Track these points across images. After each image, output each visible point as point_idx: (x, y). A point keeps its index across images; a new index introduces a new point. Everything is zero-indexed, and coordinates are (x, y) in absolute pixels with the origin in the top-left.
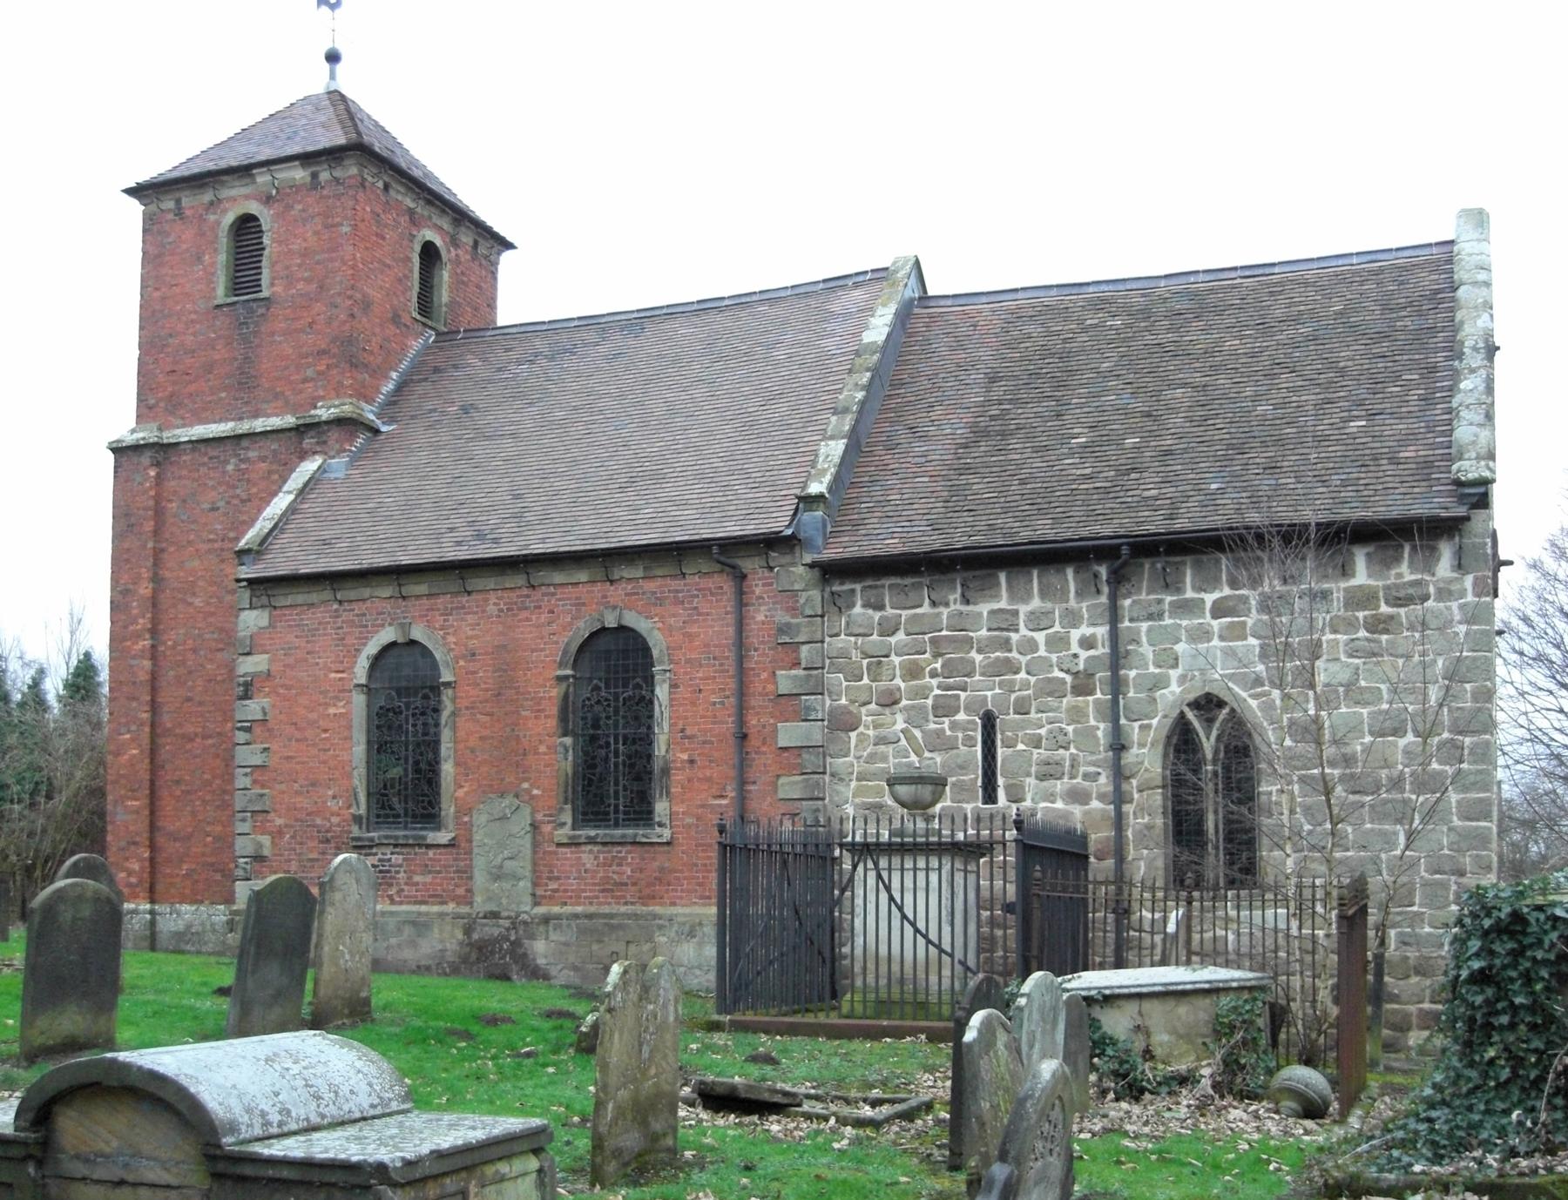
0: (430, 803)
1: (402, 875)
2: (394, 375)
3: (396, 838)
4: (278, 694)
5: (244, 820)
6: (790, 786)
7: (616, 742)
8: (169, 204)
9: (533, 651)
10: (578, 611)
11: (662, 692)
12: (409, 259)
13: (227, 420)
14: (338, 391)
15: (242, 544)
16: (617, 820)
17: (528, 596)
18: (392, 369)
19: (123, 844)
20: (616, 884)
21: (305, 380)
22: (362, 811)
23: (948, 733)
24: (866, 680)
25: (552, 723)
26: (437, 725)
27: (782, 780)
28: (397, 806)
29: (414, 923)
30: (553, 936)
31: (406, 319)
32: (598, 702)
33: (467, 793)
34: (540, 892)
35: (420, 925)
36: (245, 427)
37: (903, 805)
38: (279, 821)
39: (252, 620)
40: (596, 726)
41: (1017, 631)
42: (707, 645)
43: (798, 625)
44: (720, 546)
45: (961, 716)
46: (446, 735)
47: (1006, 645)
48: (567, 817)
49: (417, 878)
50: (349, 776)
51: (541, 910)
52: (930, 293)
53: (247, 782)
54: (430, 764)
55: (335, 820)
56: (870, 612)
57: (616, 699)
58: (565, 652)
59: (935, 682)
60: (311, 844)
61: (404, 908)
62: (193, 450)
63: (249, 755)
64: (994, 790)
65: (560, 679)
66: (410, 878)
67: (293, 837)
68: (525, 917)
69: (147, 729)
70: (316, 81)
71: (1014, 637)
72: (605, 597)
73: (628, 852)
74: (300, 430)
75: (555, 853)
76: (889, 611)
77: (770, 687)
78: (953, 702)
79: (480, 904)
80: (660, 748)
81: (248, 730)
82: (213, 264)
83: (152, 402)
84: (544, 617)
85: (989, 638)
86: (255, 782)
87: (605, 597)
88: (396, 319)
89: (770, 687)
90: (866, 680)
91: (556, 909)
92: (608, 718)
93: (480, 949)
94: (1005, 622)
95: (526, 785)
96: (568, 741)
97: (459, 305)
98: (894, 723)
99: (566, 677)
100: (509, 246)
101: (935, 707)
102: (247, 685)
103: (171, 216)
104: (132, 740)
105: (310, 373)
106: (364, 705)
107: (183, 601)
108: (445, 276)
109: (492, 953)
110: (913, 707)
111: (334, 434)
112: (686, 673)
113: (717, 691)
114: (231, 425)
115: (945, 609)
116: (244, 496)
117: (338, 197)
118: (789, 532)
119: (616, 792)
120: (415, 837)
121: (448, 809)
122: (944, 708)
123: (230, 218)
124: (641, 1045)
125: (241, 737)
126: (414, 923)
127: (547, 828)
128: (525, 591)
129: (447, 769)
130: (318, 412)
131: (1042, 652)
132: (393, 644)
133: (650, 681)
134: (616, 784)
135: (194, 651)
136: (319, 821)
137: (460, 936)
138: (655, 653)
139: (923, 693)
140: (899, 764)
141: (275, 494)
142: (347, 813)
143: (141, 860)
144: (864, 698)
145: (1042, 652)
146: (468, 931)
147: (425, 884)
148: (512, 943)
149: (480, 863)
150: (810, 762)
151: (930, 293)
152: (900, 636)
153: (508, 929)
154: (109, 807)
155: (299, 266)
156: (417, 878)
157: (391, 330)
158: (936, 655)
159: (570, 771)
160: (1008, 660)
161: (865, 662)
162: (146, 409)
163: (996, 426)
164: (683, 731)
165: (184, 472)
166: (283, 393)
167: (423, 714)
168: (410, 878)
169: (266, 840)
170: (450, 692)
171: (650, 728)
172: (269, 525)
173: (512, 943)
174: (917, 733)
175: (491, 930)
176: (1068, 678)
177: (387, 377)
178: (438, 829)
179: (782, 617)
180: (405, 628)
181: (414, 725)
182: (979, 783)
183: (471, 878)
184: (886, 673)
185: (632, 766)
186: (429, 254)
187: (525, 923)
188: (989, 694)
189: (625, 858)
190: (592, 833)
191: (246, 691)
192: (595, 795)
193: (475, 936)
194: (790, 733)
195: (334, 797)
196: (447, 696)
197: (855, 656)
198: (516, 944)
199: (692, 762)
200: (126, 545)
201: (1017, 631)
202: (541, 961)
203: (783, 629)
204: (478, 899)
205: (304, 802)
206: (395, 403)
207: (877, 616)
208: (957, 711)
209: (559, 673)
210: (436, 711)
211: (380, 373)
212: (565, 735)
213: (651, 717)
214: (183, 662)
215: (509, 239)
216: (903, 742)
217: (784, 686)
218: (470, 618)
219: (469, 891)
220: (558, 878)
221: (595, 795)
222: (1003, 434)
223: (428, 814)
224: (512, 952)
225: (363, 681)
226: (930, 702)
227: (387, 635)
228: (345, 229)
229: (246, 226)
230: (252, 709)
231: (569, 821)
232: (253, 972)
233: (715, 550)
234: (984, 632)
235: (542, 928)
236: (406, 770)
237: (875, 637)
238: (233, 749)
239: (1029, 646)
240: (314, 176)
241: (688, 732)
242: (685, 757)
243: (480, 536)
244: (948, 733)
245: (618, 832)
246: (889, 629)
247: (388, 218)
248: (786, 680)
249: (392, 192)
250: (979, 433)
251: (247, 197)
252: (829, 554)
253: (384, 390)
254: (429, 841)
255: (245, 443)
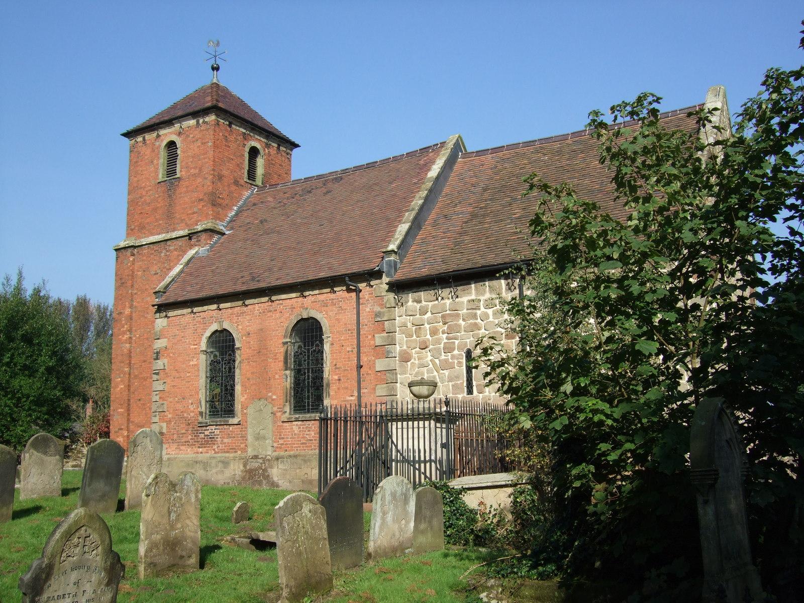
0: (231, 405)
1: (219, 439)
2: (235, 208)
3: (216, 422)
4: (170, 357)
5: (155, 416)
6: (381, 390)
7: (308, 372)
8: (140, 139)
9: (274, 331)
10: (292, 311)
11: (327, 347)
12: (243, 155)
13: (162, 233)
14: (207, 216)
15: (157, 290)
16: (309, 409)
17: (271, 306)
18: (233, 205)
19: (117, 429)
20: (308, 440)
21: (194, 213)
22: (203, 409)
23: (450, 361)
24: (415, 337)
25: (281, 364)
26: (234, 368)
27: (379, 386)
28: (218, 407)
29: (223, 462)
30: (280, 466)
31: (242, 182)
32: (301, 354)
33: (246, 399)
34: (275, 445)
35: (226, 464)
36: (168, 236)
37: (414, 395)
38: (170, 416)
39: (161, 322)
40: (300, 365)
41: (479, 309)
42: (346, 324)
43: (383, 312)
44: (349, 277)
45: (456, 352)
46: (237, 372)
47: (475, 316)
48: (287, 409)
49: (226, 440)
50: (197, 393)
51: (275, 454)
52: (468, 151)
53: (157, 398)
54: (232, 387)
55: (192, 414)
56: (415, 304)
57: (308, 352)
58: (286, 332)
59: (445, 336)
60: (182, 426)
61: (219, 455)
62: (148, 248)
63: (158, 386)
64: (472, 387)
65: (285, 343)
66: (222, 441)
67: (175, 423)
68: (269, 457)
69: (127, 376)
70: (207, 78)
71: (479, 312)
72: (303, 304)
73: (313, 425)
74: (190, 236)
75: (282, 426)
76: (424, 303)
77: (372, 342)
78: (452, 346)
79: (250, 452)
80: (326, 375)
81: (157, 374)
82: (157, 164)
83: (133, 227)
84: (278, 315)
85: (467, 313)
86: (160, 398)
87: (303, 304)
88: (236, 183)
89: (372, 342)
90: (415, 337)
91: (282, 453)
92: (305, 361)
93: (250, 473)
94: (474, 305)
95: (270, 394)
96: (288, 372)
97: (270, 174)
98: (427, 357)
99: (287, 343)
100: (297, 146)
101: (444, 349)
102: (158, 353)
103: (141, 144)
104: (121, 381)
105: (195, 210)
106: (205, 359)
107: (143, 316)
108: (260, 162)
109: (255, 475)
110: (435, 349)
111: (203, 236)
112: (337, 338)
113: (350, 346)
114: (164, 235)
115: (446, 299)
116: (168, 267)
117: (207, 130)
118: (377, 268)
119: (308, 396)
120: (224, 421)
121: (238, 407)
122: (448, 349)
123: (165, 143)
124: (169, 513)
125: (155, 377)
126: (223, 462)
127: (279, 414)
128: (270, 303)
129: (238, 388)
130: (198, 227)
131: (491, 319)
132: (216, 331)
133: (322, 341)
134: (308, 392)
135: (147, 339)
136: (185, 415)
137: (242, 467)
138: (324, 329)
139: (438, 342)
140: (430, 377)
141: (176, 265)
142: (197, 411)
143: (124, 437)
144: (413, 345)
145: (491, 319)
146: (245, 466)
147: (228, 443)
148: (263, 470)
149: (250, 431)
150: (388, 377)
151: (468, 151)
152: (429, 314)
153: (261, 464)
154: (111, 413)
155: (192, 162)
156: (226, 440)
157: (233, 188)
158: (445, 324)
159: (288, 387)
160: (475, 323)
161: (414, 328)
162: (130, 231)
163: (482, 212)
164: (336, 365)
165: (145, 258)
166: (184, 219)
167: (229, 363)
168: (222, 441)
169: (164, 425)
170: (239, 351)
171: (322, 365)
172: (170, 280)
173: (263, 470)
174: (437, 361)
175: (254, 464)
176: (503, 331)
177: (231, 209)
178: (233, 417)
179: (377, 309)
180: (221, 323)
181: (225, 368)
182: (465, 384)
183: (247, 440)
184: (422, 332)
185: (315, 383)
186: (254, 152)
187: (269, 460)
188: (468, 340)
189: (311, 428)
190: (297, 416)
191: (157, 356)
192: (300, 398)
193: (248, 467)
194: (381, 364)
195: (192, 404)
196: (238, 353)
197: (409, 325)
198: (265, 470)
199: (339, 380)
200: (120, 292)
201: (479, 309)
202: (275, 479)
203: (378, 315)
204: (250, 450)
205: (180, 407)
206: (234, 221)
207: (418, 306)
208: (454, 349)
209: (285, 340)
210: (234, 361)
211: (229, 207)
212: (286, 370)
213: (322, 359)
214: (143, 344)
215: (296, 142)
216: (431, 366)
217: (378, 341)
218: (248, 317)
219: (246, 446)
220: (283, 438)
221: (300, 398)
222: (484, 216)
223: (229, 411)
224: (263, 475)
225: (204, 348)
226: (442, 346)
227: (215, 327)
228: (210, 144)
229: (171, 145)
230: (159, 364)
231: (288, 411)
232: (90, 485)
233: (347, 279)
234: (465, 311)
235: (276, 463)
236: (221, 390)
237: (418, 316)
238: (151, 383)
239: (485, 317)
240: (198, 122)
241: (338, 366)
242: (336, 377)
243: (253, 279)
244: (450, 361)
245: (308, 415)
246: (423, 312)
247: (232, 138)
248: (379, 339)
249: (233, 126)
250: (474, 216)
251: (171, 133)
252: (399, 276)
253: (230, 215)
254: (230, 423)
255: (169, 243)
